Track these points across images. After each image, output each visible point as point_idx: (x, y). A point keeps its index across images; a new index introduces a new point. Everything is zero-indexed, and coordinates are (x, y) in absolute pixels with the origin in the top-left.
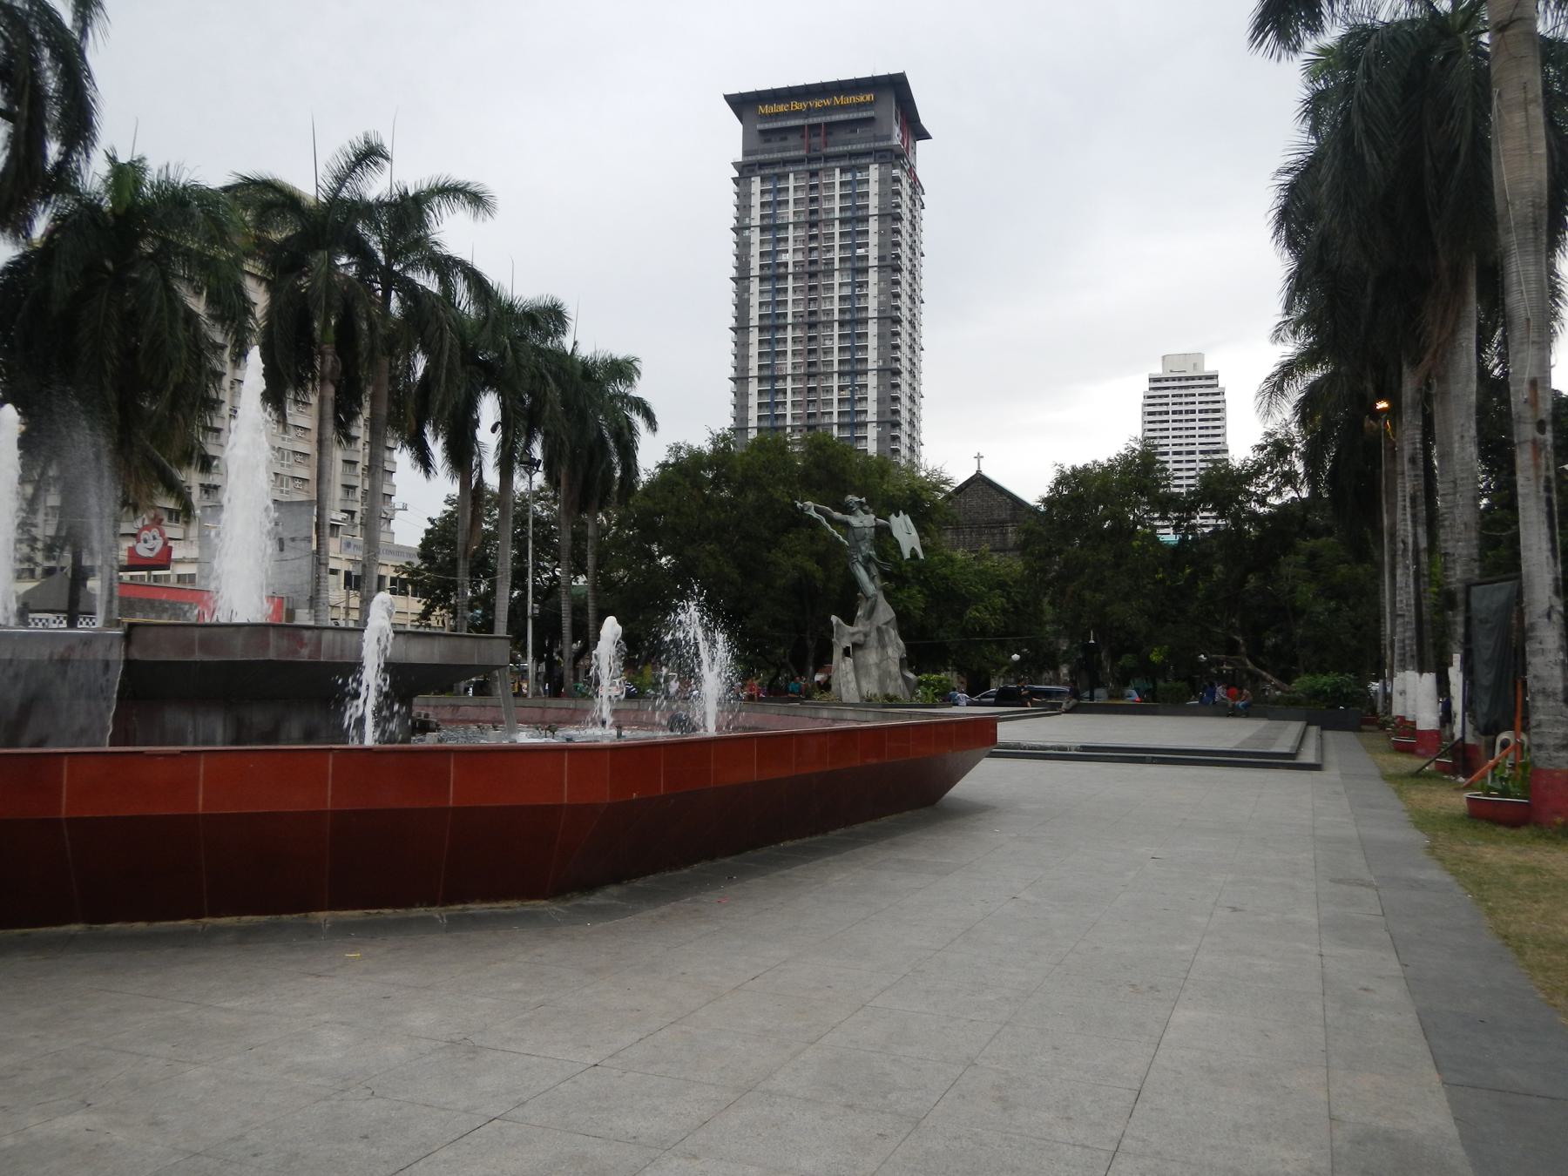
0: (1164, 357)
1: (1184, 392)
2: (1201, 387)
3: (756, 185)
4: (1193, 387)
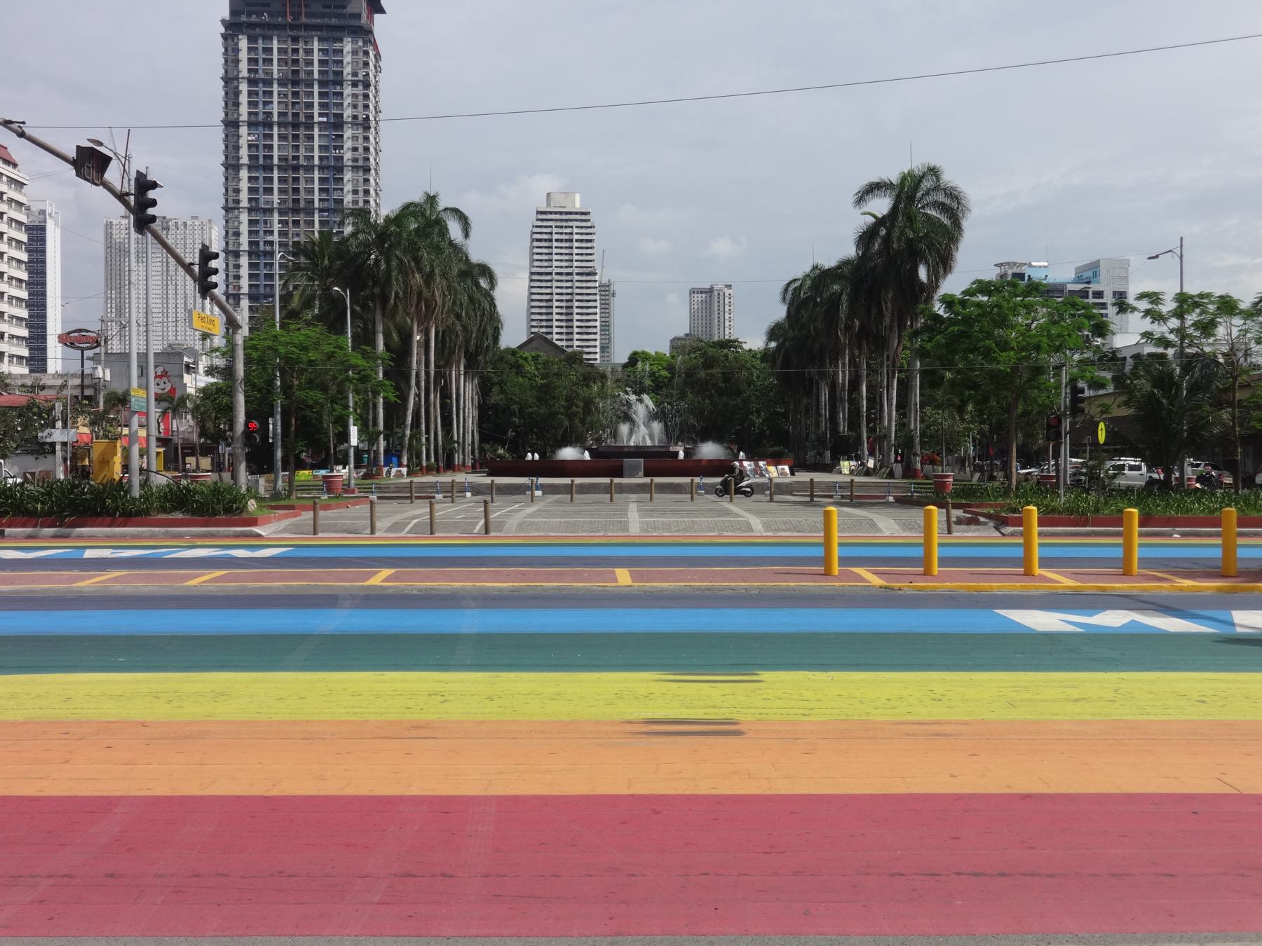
0: (548, 194)
1: (564, 224)
2: (577, 220)
3: (243, 43)
4: (571, 220)
